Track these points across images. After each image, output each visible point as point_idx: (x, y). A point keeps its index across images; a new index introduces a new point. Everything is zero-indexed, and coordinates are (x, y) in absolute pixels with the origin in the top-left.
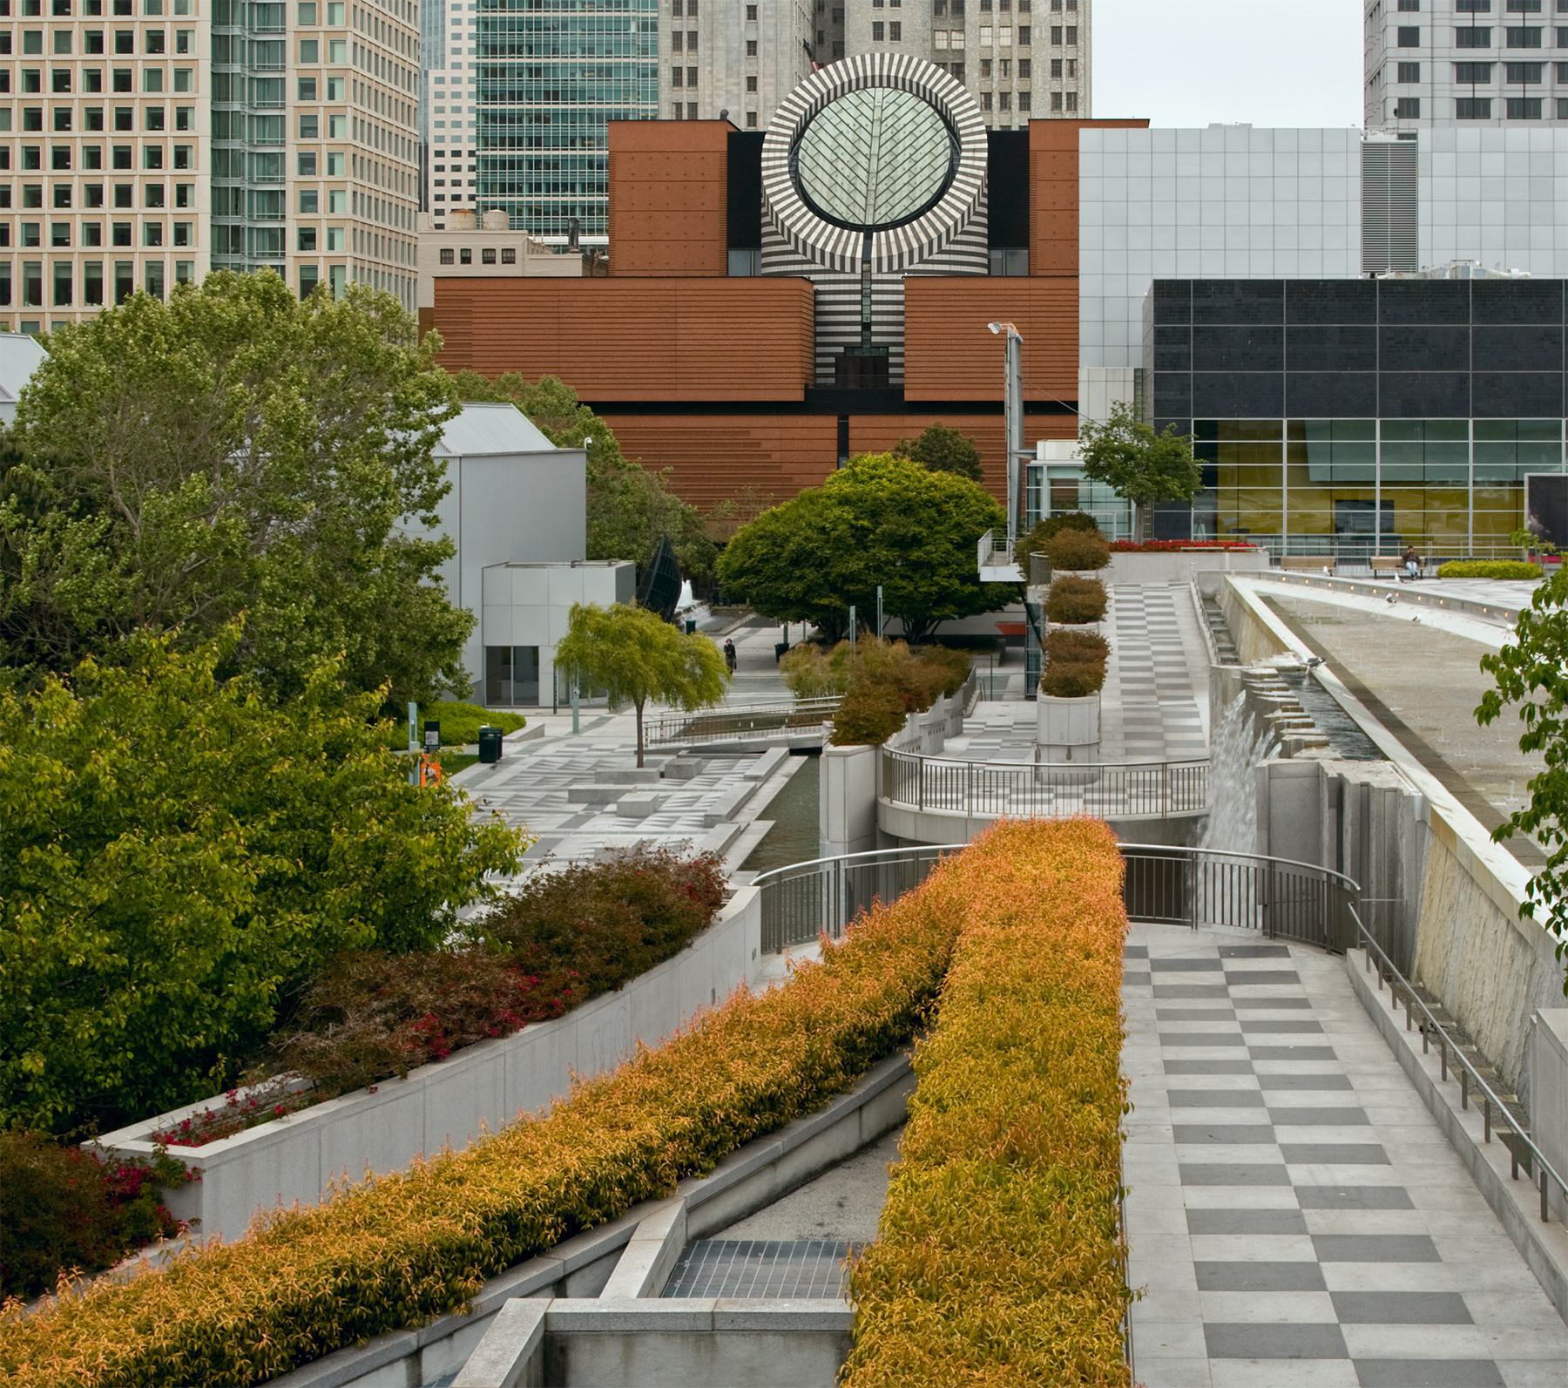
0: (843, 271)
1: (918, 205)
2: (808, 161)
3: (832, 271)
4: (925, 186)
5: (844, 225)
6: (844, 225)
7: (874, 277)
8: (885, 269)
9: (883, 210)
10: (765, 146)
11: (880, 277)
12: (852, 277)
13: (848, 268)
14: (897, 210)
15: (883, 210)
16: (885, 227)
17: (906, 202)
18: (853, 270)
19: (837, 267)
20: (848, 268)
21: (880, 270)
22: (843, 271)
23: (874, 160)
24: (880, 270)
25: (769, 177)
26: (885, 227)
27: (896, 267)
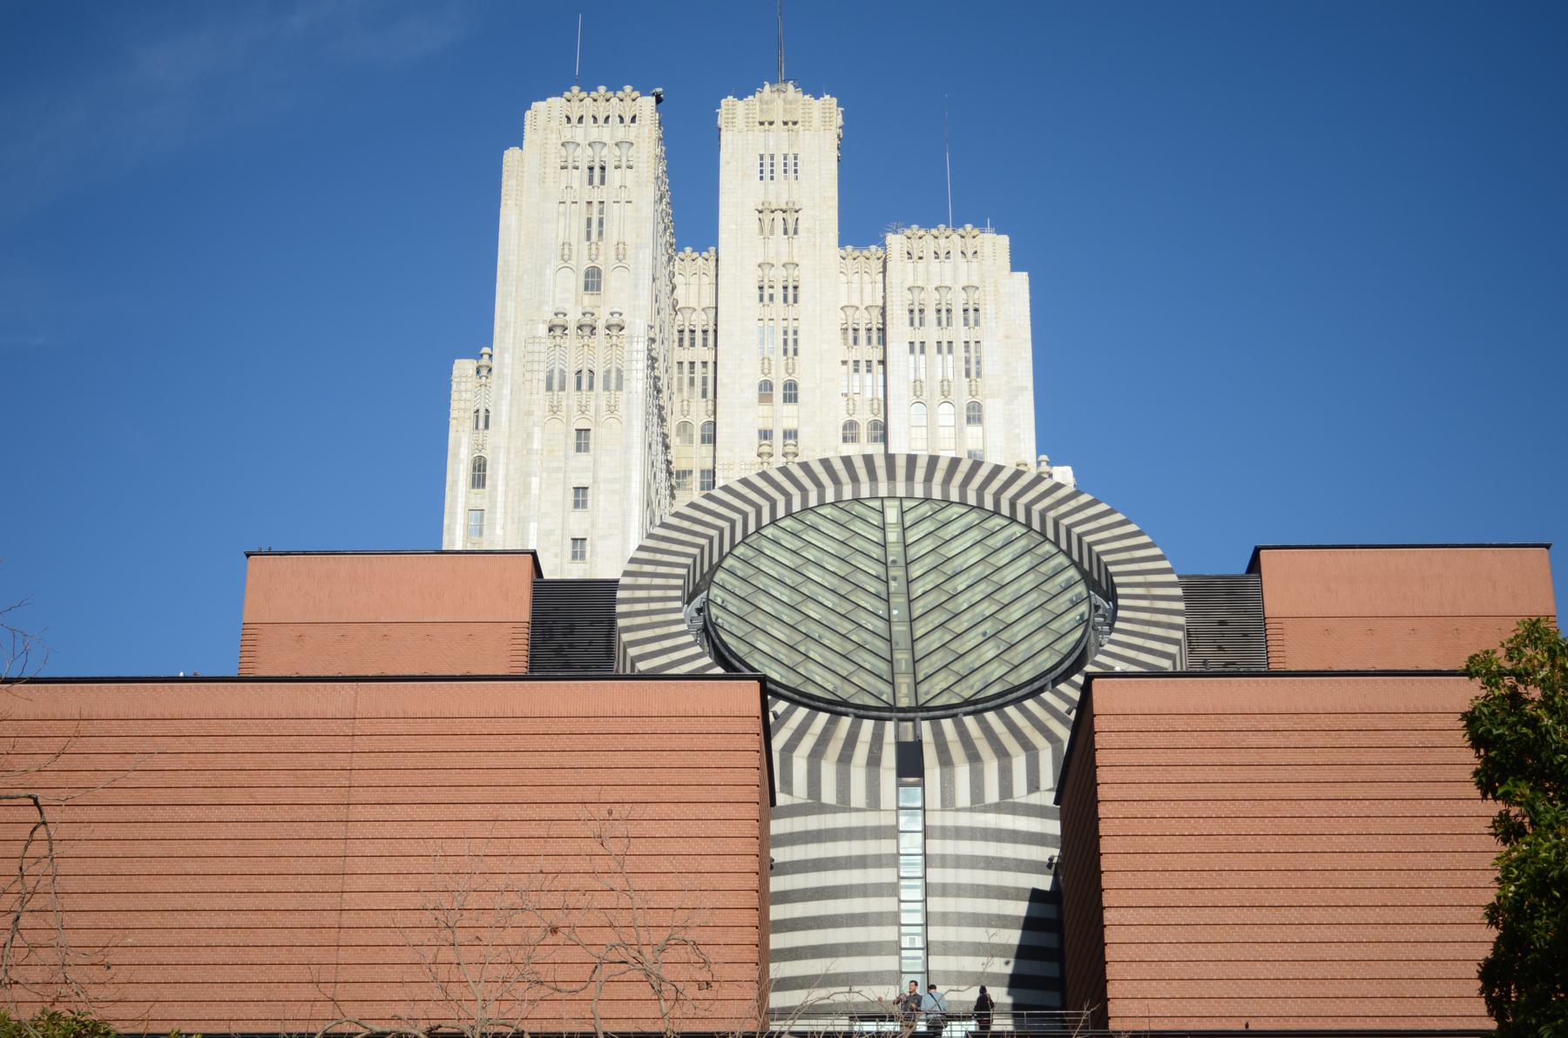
0: (843, 805)
1: (1026, 673)
2: (734, 605)
3: (815, 806)
4: (1040, 640)
5: (835, 707)
6: (835, 707)
7: (935, 819)
8: (963, 796)
9: (940, 682)
10: (620, 594)
11: (950, 819)
12: (871, 819)
13: (858, 796)
14: (976, 682)
15: (940, 682)
16: (950, 710)
17: (997, 670)
18: (874, 803)
19: (829, 795)
20: (858, 796)
21: (947, 802)
22: (843, 805)
23: (898, 601)
24: (947, 802)
25: (628, 629)
26: (950, 710)
27: (992, 794)
